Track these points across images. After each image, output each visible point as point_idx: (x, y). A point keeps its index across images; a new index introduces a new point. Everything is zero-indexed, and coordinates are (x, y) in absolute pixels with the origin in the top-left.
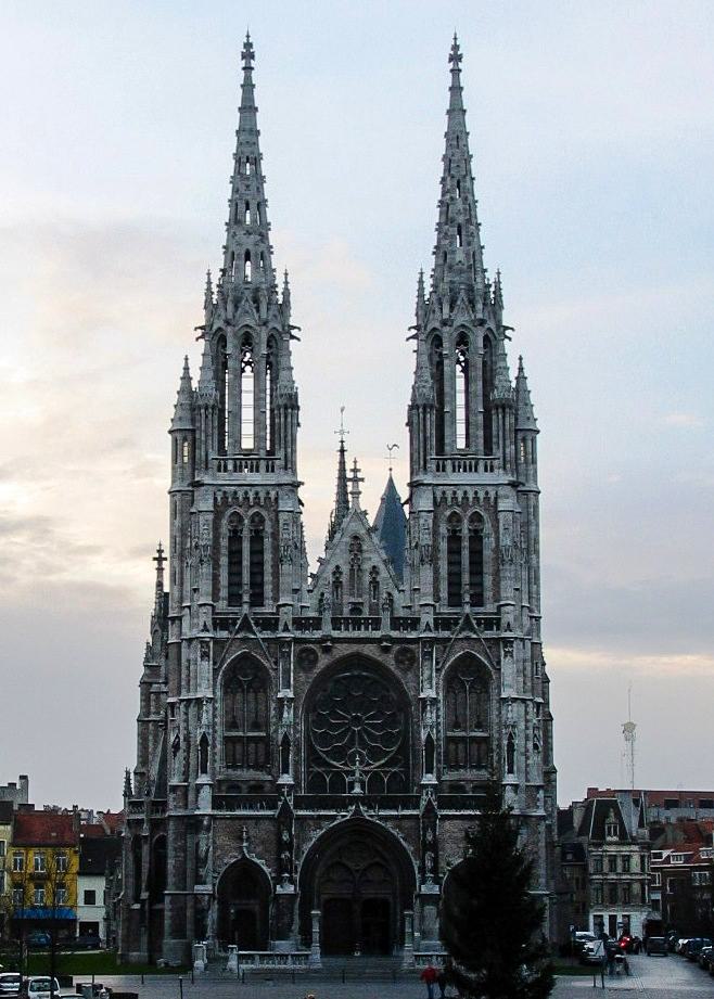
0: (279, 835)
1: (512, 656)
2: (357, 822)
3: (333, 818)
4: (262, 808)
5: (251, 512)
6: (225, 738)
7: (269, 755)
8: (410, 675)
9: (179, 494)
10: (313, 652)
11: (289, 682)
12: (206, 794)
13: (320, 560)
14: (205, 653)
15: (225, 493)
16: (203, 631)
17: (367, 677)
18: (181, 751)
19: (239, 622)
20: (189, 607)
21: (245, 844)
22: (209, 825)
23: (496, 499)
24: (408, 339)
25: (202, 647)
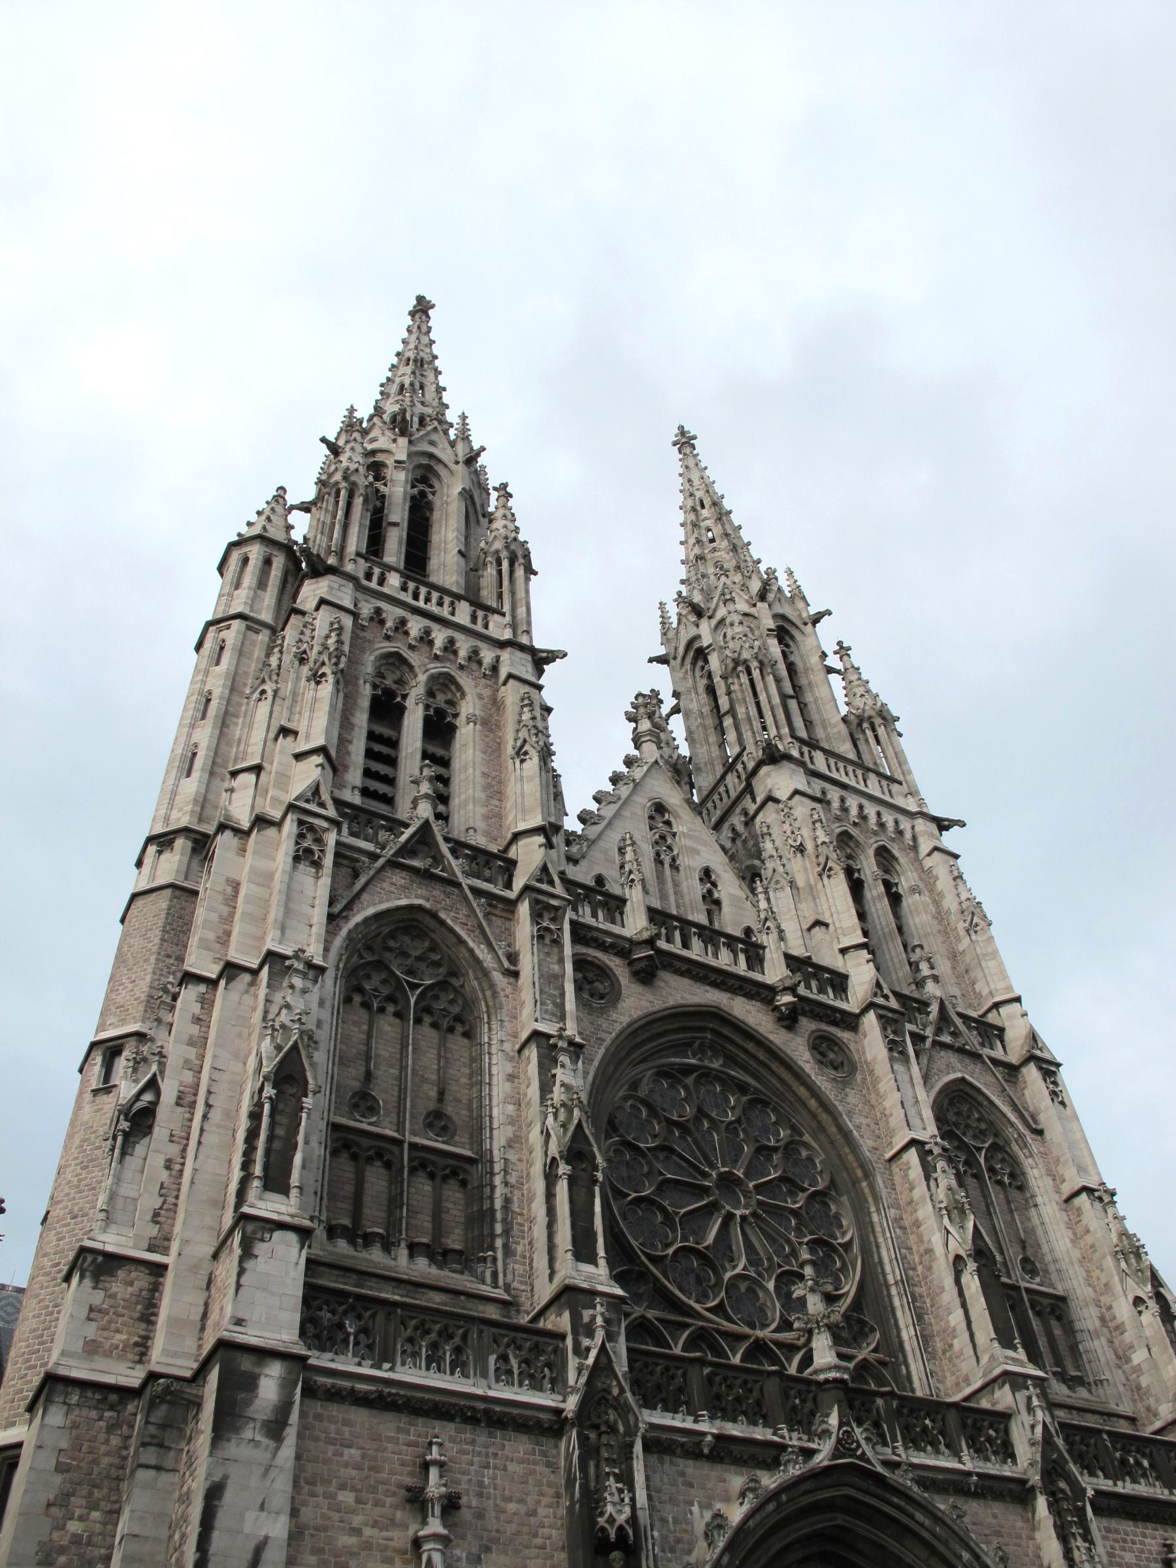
0: (592, 1500)
1: (1062, 1103)
2: (848, 1470)
3: (771, 1456)
4: (504, 1374)
5: (436, 668)
6: (335, 1127)
7: (481, 1218)
8: (853, 1097)
9: (236, 624)
10: (604, 973)
11: (562, 1006)
12: (283, 1265)
13: (583, 818)
14: (308, 851)
15: (378, 611)
16: (307, 801)
17: (742, 1088)
18: (160, 1131)
19: (408, 833)
20: (257, 769)
21: (435, 1526)
22: (284, 1409)
23: (914, 838)
24: (651, 660)
25: (301, 836)
